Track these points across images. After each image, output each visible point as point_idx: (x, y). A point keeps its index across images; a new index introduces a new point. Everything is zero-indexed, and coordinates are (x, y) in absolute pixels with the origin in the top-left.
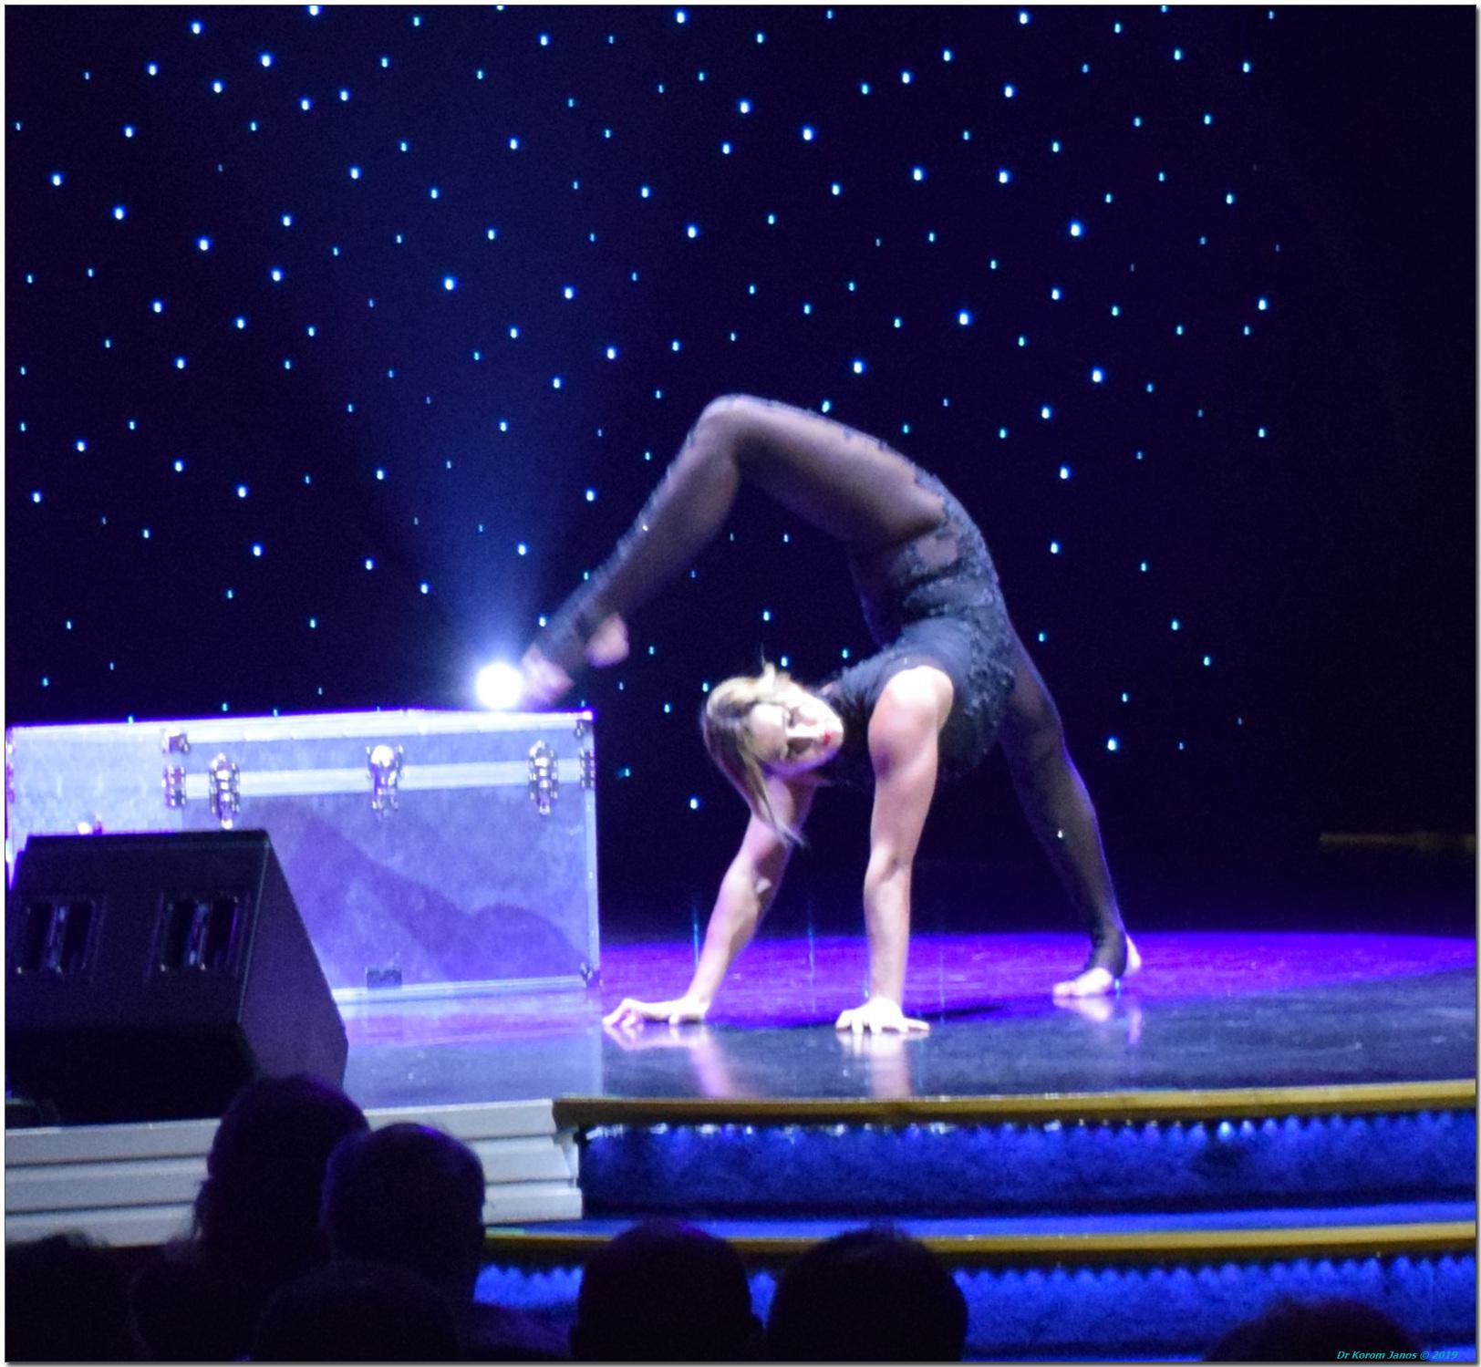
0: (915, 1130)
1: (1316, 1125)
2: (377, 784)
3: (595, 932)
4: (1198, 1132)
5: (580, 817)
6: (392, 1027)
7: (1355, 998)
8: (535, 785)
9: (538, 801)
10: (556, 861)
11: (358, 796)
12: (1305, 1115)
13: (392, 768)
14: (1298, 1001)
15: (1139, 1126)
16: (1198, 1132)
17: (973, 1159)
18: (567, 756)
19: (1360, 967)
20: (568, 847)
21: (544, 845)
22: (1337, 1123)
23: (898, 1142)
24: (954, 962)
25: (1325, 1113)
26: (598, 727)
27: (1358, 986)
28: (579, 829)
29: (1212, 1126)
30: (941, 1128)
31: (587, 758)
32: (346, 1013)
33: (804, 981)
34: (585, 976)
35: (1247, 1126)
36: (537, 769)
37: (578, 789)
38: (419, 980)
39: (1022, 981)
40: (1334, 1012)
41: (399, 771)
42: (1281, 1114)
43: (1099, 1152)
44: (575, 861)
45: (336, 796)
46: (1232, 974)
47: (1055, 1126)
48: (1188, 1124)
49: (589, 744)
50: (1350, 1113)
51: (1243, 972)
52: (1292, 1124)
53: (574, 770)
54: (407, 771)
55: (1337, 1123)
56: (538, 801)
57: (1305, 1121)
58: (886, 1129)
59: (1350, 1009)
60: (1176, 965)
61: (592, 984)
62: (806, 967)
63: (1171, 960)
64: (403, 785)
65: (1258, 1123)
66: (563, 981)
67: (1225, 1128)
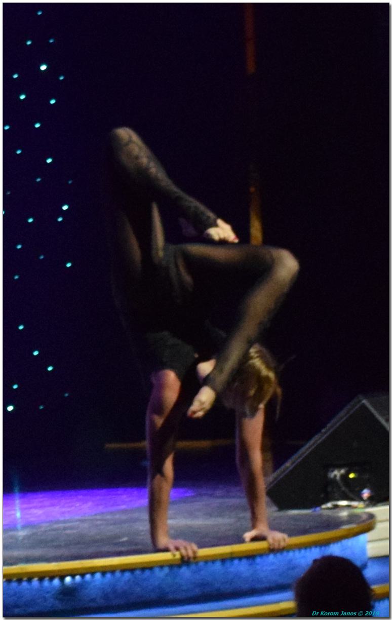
1: (108, 576)
4: (56, 582)
7: (124, 517)
12: (104, 571)
14: (97, 520)
19: (124, 503)
22: (118, 574)
25: (112, 570)
27: (124, 511)
29: (62, 578)
35: (78, 578)
40: (114, 524)
42: (93, 571)
46: (69, 509)
48: (52, 578)
50: (124, 569)
51: (73, 508)
52: (98, 576)
55: (118, 574)
57: (104, 573)
59: (122, 522)
60: (41, 507)
63: (40, 504)
65: (83, 576)
67: (68, 579)
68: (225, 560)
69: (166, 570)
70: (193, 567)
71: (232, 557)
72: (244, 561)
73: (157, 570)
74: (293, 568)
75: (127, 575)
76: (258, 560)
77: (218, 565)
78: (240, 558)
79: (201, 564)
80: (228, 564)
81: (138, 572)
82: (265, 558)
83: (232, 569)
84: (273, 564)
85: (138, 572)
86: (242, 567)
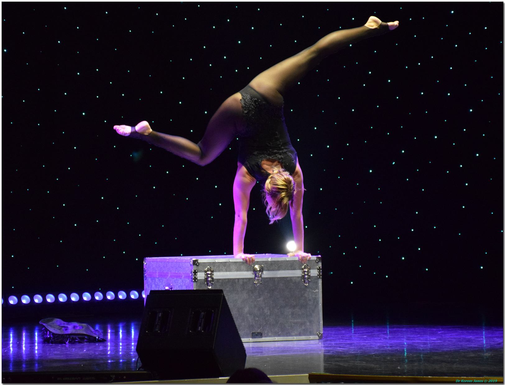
2: (256, 276)
3: (322, 322)
5: (317, 288)
6: (260, 350)
8: (303, 277)
9: (304, 281)
10: (310, 300)
11: (250, 279)
13: (260, 271)
18: (313, 269)
20: (314, 296)
21: (306, 295)
24: (433, 334)
26: (323, 260)
28: (317, 290)
31: (319, 269)
32: (245, 345)
33: (386, 338)
34: (318, 335)
36: (305, 271)
37: (316, 278)
38: (267, 336)
39: (454, 340)
41: (262, 272)
44: (315, 300)
45: (243, 279)
49: (320, 265)
53: (314, 273)
54: (264, 272)
56: (304, 281)
61: (320, 338)
62: (386, 334)
64: (263, 276)
66: (312, 337)
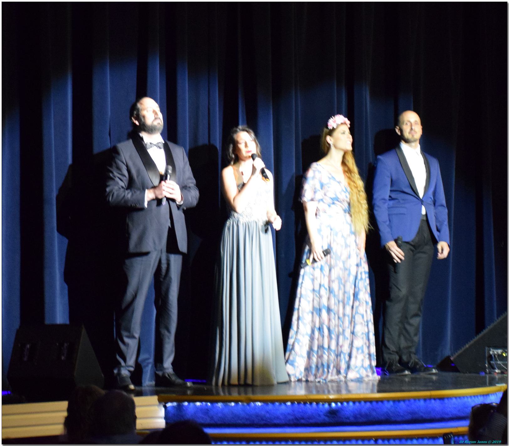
0: (252, 404)
1: (357, 404)
15: (311, 403)
16: (326, 405)
17: (267, 412)
22: (363, 403)
23: (248, 407)
30: (259, 404)
35: (339, 404)
43: (300, 410)
47: (289, 404)
52: (351, 404)
55: (363, 403)
58: (245, 404)
65: (342, 403)
68: (425, 399)
69: (391, 403)
70: (407, 402)
71: (430, 398)
72: (438, 401)
73: (386, 403)
74: (466, 408)
75: (368, 404)
76: (446, 401)
77: (422, 402)
78: (435, 399)
79: (412, 401)
80: (428, 402)
81: (374, 403)
82: (450, 400)
83: (431, 405)
84: (454, 404)
85: (374, 403)
86: (436, 405)
